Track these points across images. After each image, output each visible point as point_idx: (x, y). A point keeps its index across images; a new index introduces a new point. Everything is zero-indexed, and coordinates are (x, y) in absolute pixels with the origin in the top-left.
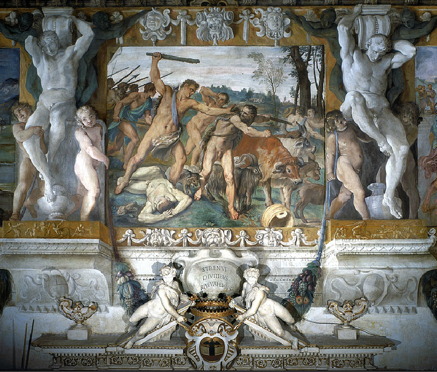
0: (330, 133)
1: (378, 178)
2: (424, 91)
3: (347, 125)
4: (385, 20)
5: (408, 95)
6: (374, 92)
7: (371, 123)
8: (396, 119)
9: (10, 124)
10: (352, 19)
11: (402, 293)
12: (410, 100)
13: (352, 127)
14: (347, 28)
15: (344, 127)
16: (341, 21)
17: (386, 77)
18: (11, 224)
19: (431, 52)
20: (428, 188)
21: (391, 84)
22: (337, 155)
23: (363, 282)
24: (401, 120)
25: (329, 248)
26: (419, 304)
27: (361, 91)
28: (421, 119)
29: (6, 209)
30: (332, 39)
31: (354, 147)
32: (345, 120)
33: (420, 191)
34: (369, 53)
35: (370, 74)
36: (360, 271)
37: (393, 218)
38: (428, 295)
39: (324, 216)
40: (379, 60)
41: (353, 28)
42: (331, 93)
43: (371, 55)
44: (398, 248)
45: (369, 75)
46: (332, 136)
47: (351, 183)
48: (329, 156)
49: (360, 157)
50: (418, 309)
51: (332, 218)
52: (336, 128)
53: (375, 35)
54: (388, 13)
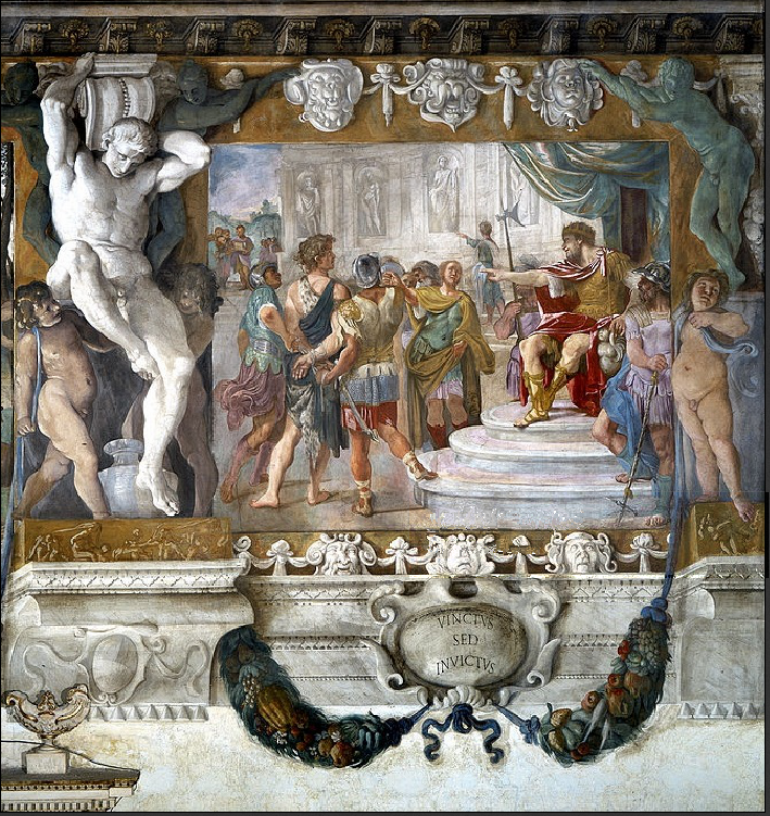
0: (23, 331)
1: (127, 427)
2: (228, 240)
3: (61, 313)
4: (145, 86)
5: (192, 250)
6: (120, 243)
7: (113, 311)
8: (165, 301)
10: (72, 84)
11: (176, 678)
12: (197, 260)
13: (72, 318)
14: (63, 106)
15: (54, 318)
16: (47, 91)
17: (144, 211)
19: (243, 156)
20: (235, 451)
21: (155, 225)
22: (40, 378)
23: (92, 653)
24: (177, 303)
25: (20, 579)
26: (212, 701)
27: (91, 242)
28: (221, 300)
30: (29, 129)
31: (75, 361)
32: (58, 304)
33: (217, 456)
34: (109, 159)
35: (111, 205)
36: (86, 630)
37: (159, 515)
38: (232, 680)
39: (10, 511)
40: (131, 174)
41: (74, 105)
42: (27, 247)
43: (114, 163)
44: (168, 580)
45: (109, 206)
46: (28, 338)
47: (69, 438)
48: (23, 381)
49: (88, 383)
50: (211, 711)
51: (27, 515)
52: (38, 320)
53: (120, 121)
54: (152, 71)
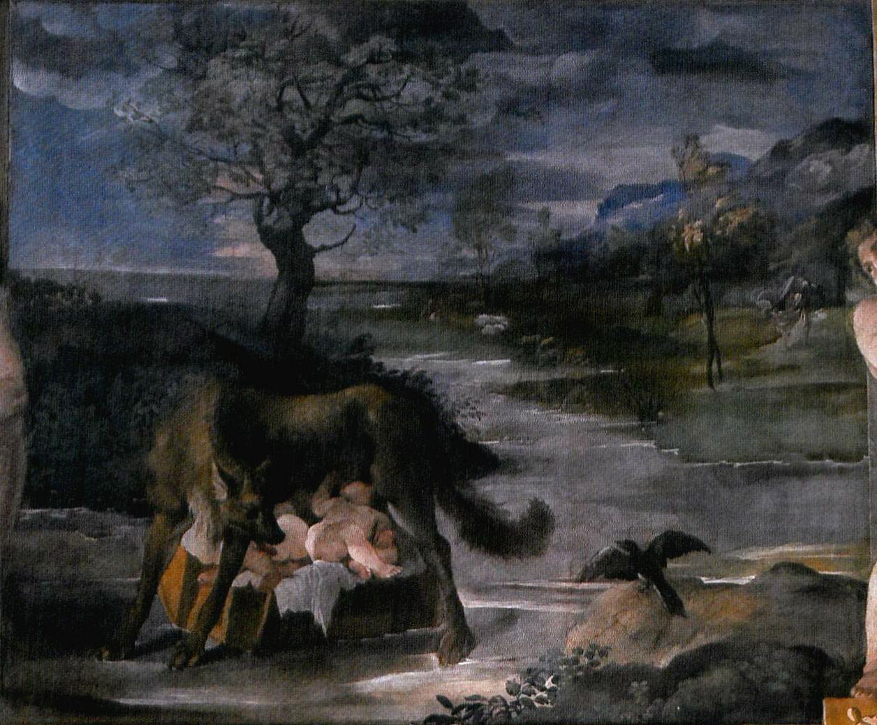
9: (841, 302)
18: (858, 713)
29: (838, 651)
